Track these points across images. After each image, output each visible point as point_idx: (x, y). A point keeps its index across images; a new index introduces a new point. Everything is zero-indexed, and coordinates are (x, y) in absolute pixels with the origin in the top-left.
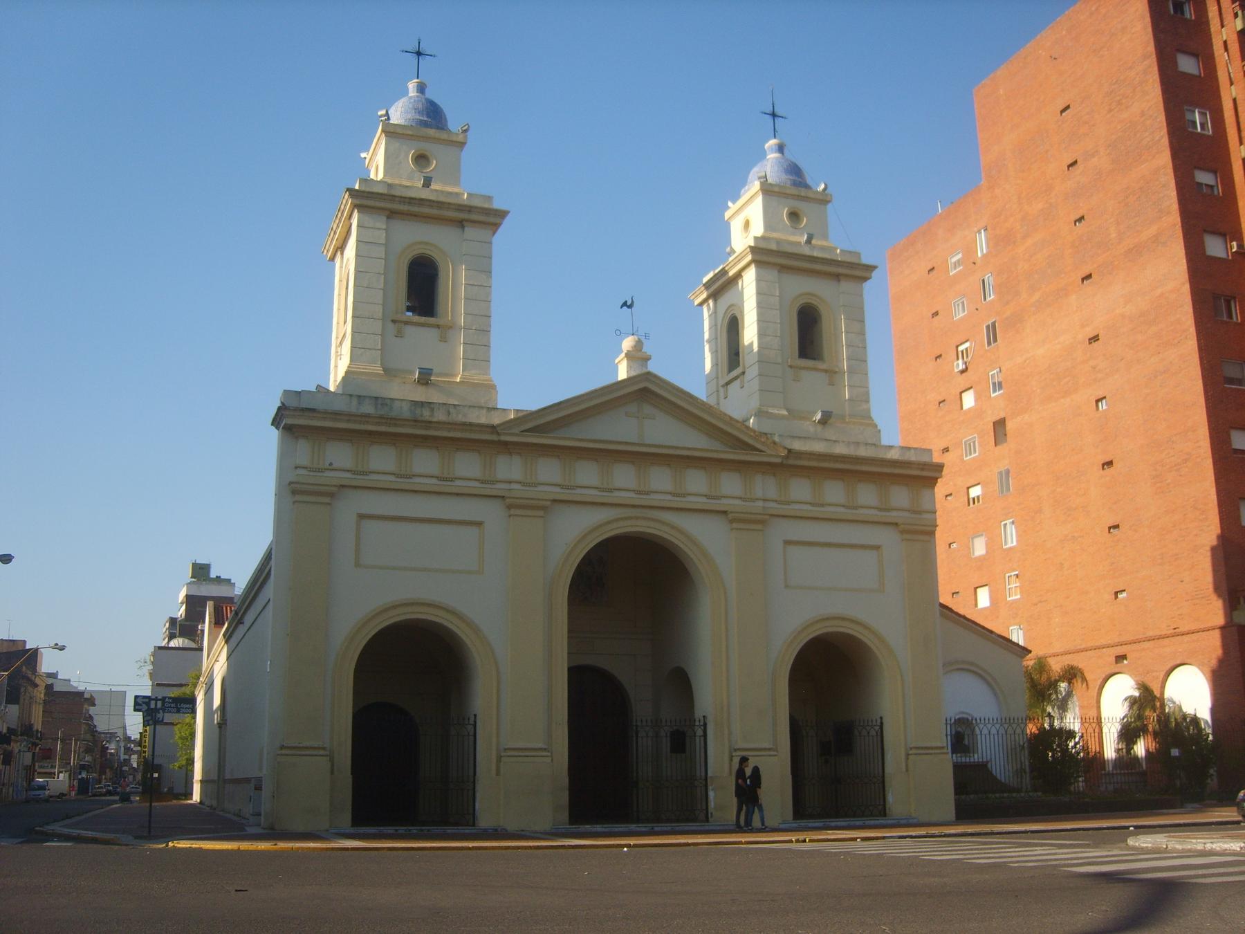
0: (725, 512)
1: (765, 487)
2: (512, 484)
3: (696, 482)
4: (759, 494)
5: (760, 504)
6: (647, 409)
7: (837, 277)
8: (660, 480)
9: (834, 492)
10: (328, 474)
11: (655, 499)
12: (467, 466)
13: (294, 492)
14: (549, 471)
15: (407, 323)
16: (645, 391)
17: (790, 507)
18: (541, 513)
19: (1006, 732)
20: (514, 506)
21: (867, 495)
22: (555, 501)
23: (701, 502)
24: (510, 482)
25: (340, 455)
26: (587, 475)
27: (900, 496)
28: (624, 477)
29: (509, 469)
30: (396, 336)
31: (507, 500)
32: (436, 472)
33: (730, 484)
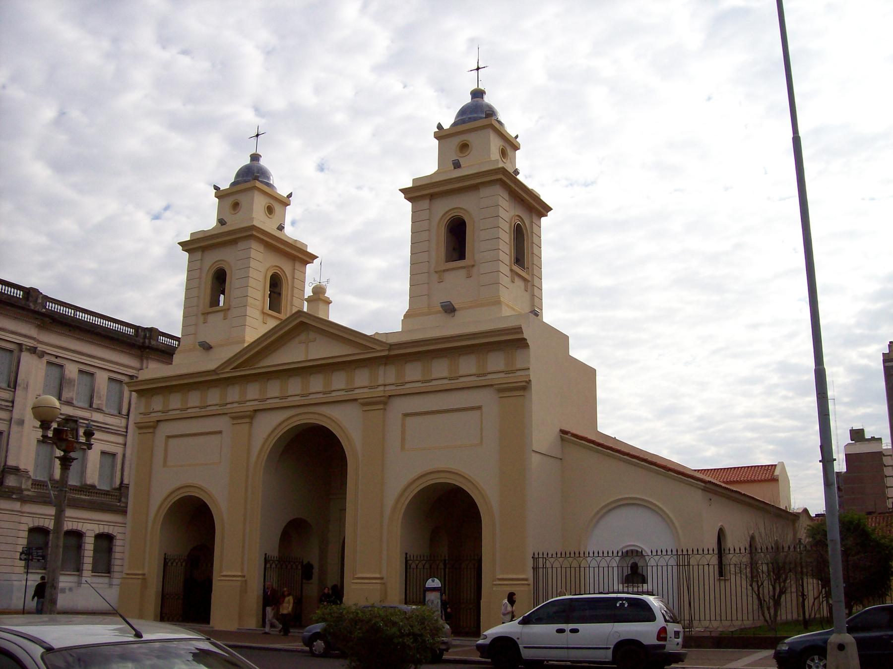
0: (356, 400)
1: (388, 375)
2: (234, 404)
3: (339, 381)
4: (381, 382)
5: (381, 388)
6: (312, 335)
7: (475, 187)
8: (316, 384)
9: (440, 369)
10: (153, 415)
11: (313, 399)
12: (214, 397)
13: (140, 428)
14: (253, 391)
15: (208, 313)
16: (302, 323)
17: (516, 375)
18: (381, 407)
19: (417, 566)
20: (236, 417)
21: (468, 366)
22: (255, 411)
23: (342, 395)
24: (233, 403)
25: (157, 403)
26: (274, 389)
27: (496, 362)
28: (294, 386)
29: (233, 394)
30: (204, 323)
31: (495, 386)
32: (419, 378)
33: (362, 378)
